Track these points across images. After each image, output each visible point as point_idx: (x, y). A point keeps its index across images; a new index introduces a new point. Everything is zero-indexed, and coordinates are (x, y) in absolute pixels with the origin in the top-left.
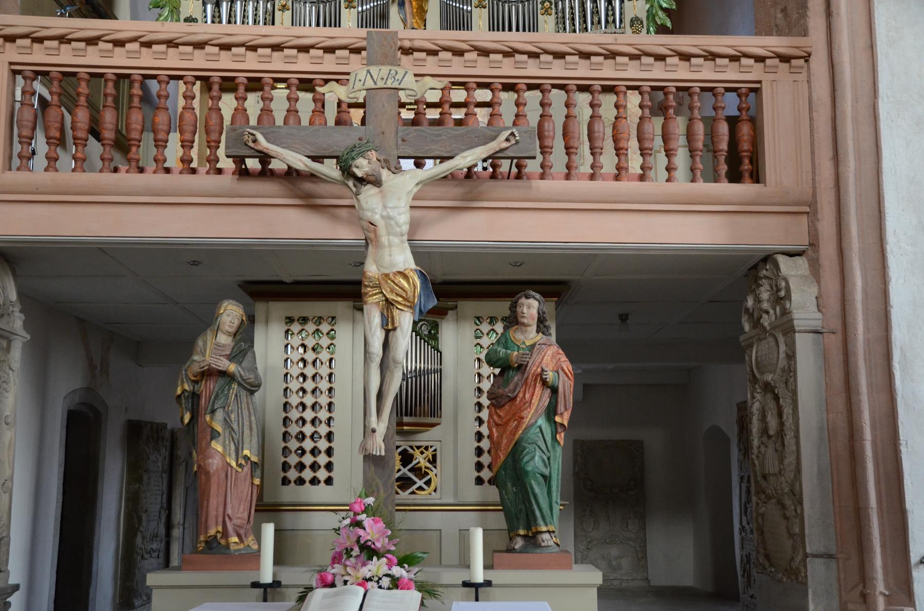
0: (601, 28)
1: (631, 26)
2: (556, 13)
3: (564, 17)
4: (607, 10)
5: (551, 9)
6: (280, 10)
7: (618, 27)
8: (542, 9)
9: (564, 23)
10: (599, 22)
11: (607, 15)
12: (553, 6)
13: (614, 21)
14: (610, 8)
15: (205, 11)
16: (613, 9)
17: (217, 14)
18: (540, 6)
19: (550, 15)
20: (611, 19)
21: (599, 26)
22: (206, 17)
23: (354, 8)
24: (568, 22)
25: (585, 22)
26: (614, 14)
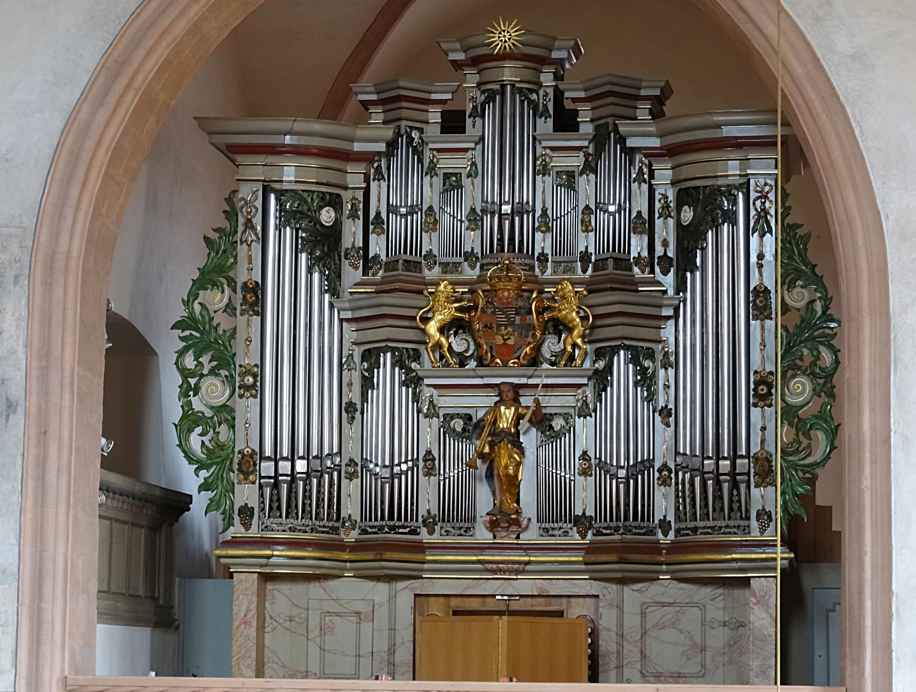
0: (724, 520)
1: (758, 521)
2: (677, 484)
3: (684, 492)
4: (731, 495)
5: (671, 479)
6: (346, 478)
7: (744, 516)
8: (658, 479)
9: (684, 500)
10: (722, 509)
11: (731, 501)
12: (673, 475)
13: (740, 508)
14: (735, 492)
15: (262, 495)
16: (739, 494)
17: (275, 498)
18: (657, 475)
19: (670, 485)
20: (736, 506)
21: (722, 513)
22: (263, 502)
23: (435, 475)
24: (688, 500)
25: (706, 505)
26: (739, 501)
